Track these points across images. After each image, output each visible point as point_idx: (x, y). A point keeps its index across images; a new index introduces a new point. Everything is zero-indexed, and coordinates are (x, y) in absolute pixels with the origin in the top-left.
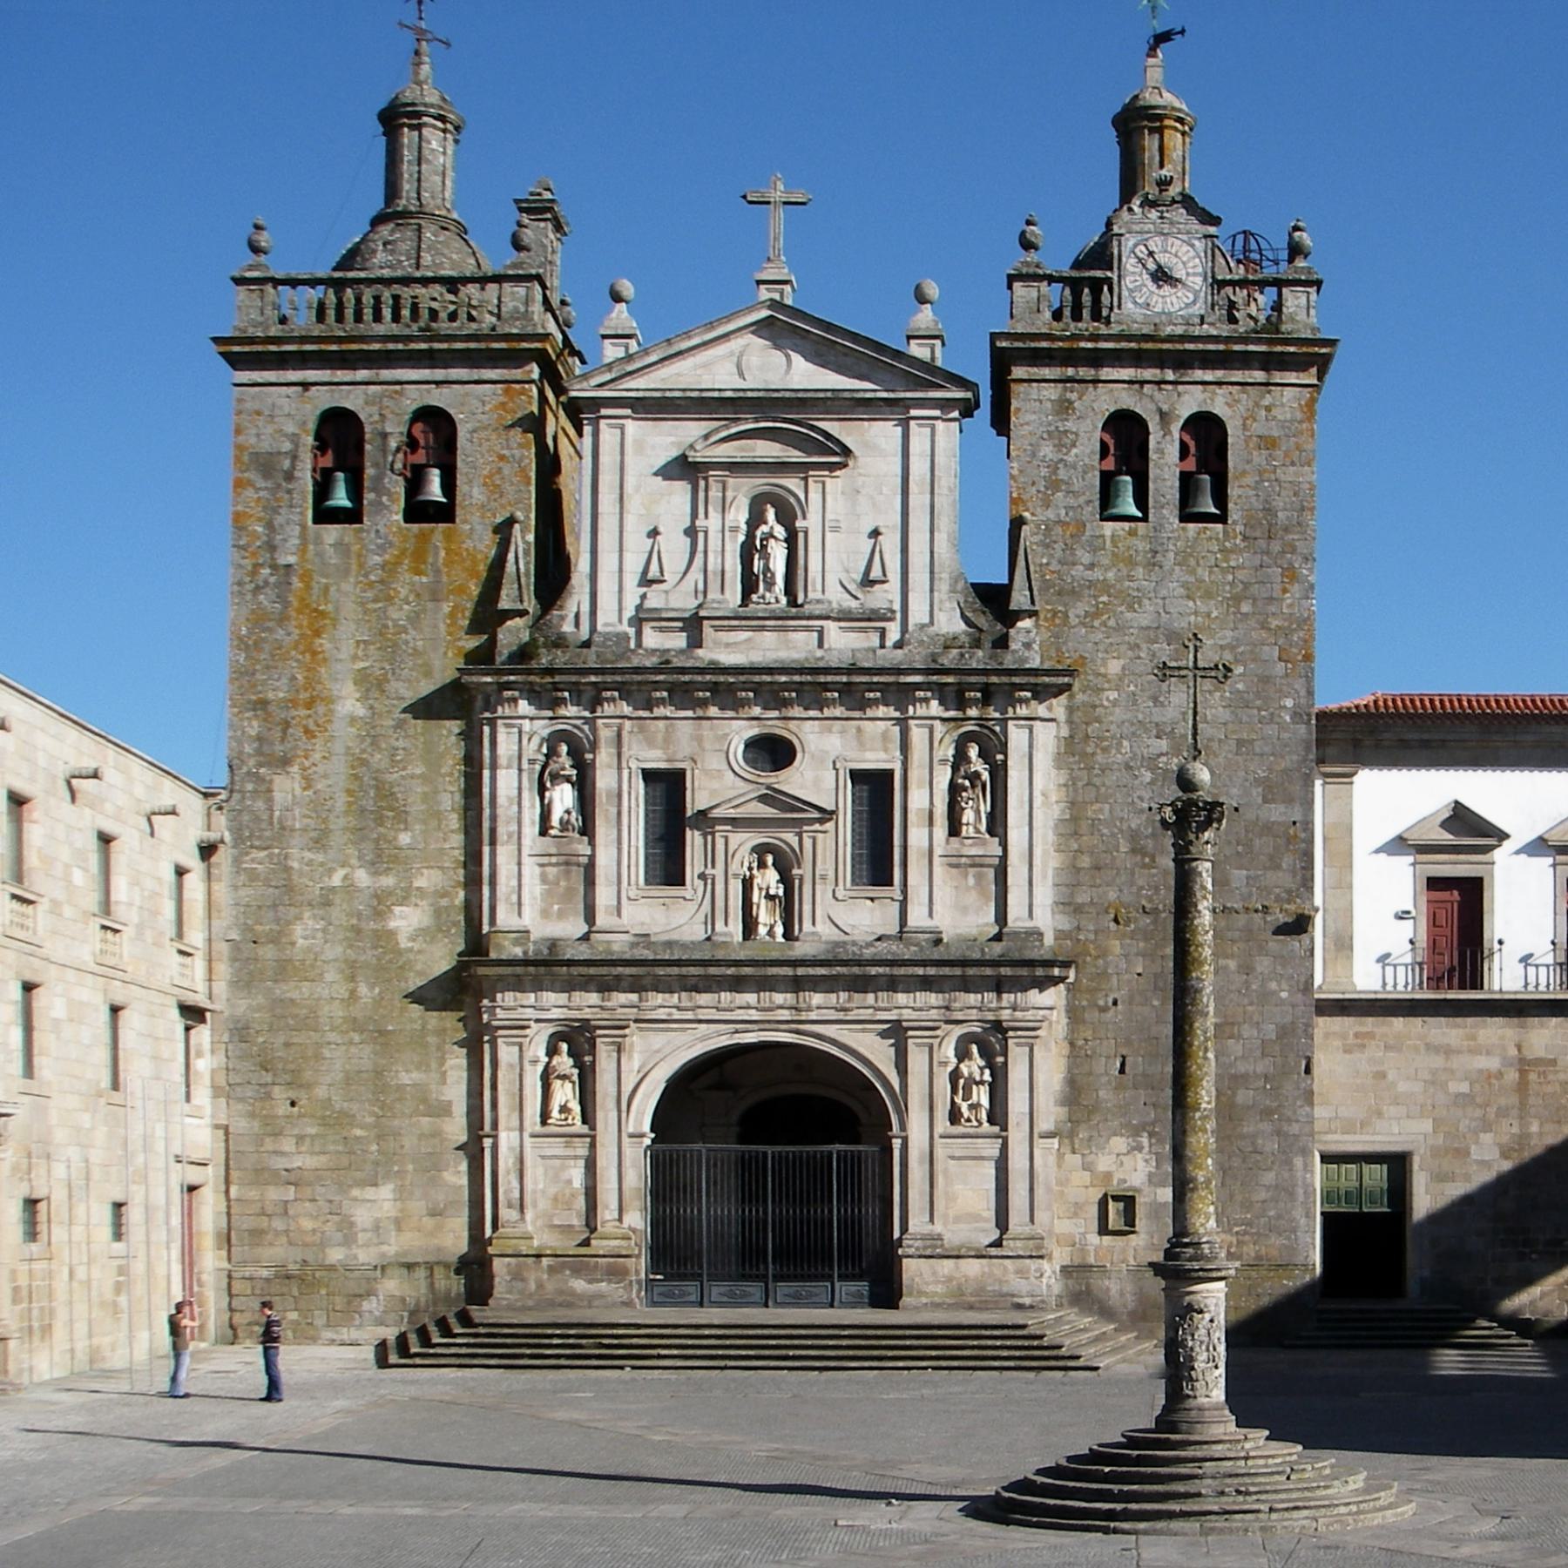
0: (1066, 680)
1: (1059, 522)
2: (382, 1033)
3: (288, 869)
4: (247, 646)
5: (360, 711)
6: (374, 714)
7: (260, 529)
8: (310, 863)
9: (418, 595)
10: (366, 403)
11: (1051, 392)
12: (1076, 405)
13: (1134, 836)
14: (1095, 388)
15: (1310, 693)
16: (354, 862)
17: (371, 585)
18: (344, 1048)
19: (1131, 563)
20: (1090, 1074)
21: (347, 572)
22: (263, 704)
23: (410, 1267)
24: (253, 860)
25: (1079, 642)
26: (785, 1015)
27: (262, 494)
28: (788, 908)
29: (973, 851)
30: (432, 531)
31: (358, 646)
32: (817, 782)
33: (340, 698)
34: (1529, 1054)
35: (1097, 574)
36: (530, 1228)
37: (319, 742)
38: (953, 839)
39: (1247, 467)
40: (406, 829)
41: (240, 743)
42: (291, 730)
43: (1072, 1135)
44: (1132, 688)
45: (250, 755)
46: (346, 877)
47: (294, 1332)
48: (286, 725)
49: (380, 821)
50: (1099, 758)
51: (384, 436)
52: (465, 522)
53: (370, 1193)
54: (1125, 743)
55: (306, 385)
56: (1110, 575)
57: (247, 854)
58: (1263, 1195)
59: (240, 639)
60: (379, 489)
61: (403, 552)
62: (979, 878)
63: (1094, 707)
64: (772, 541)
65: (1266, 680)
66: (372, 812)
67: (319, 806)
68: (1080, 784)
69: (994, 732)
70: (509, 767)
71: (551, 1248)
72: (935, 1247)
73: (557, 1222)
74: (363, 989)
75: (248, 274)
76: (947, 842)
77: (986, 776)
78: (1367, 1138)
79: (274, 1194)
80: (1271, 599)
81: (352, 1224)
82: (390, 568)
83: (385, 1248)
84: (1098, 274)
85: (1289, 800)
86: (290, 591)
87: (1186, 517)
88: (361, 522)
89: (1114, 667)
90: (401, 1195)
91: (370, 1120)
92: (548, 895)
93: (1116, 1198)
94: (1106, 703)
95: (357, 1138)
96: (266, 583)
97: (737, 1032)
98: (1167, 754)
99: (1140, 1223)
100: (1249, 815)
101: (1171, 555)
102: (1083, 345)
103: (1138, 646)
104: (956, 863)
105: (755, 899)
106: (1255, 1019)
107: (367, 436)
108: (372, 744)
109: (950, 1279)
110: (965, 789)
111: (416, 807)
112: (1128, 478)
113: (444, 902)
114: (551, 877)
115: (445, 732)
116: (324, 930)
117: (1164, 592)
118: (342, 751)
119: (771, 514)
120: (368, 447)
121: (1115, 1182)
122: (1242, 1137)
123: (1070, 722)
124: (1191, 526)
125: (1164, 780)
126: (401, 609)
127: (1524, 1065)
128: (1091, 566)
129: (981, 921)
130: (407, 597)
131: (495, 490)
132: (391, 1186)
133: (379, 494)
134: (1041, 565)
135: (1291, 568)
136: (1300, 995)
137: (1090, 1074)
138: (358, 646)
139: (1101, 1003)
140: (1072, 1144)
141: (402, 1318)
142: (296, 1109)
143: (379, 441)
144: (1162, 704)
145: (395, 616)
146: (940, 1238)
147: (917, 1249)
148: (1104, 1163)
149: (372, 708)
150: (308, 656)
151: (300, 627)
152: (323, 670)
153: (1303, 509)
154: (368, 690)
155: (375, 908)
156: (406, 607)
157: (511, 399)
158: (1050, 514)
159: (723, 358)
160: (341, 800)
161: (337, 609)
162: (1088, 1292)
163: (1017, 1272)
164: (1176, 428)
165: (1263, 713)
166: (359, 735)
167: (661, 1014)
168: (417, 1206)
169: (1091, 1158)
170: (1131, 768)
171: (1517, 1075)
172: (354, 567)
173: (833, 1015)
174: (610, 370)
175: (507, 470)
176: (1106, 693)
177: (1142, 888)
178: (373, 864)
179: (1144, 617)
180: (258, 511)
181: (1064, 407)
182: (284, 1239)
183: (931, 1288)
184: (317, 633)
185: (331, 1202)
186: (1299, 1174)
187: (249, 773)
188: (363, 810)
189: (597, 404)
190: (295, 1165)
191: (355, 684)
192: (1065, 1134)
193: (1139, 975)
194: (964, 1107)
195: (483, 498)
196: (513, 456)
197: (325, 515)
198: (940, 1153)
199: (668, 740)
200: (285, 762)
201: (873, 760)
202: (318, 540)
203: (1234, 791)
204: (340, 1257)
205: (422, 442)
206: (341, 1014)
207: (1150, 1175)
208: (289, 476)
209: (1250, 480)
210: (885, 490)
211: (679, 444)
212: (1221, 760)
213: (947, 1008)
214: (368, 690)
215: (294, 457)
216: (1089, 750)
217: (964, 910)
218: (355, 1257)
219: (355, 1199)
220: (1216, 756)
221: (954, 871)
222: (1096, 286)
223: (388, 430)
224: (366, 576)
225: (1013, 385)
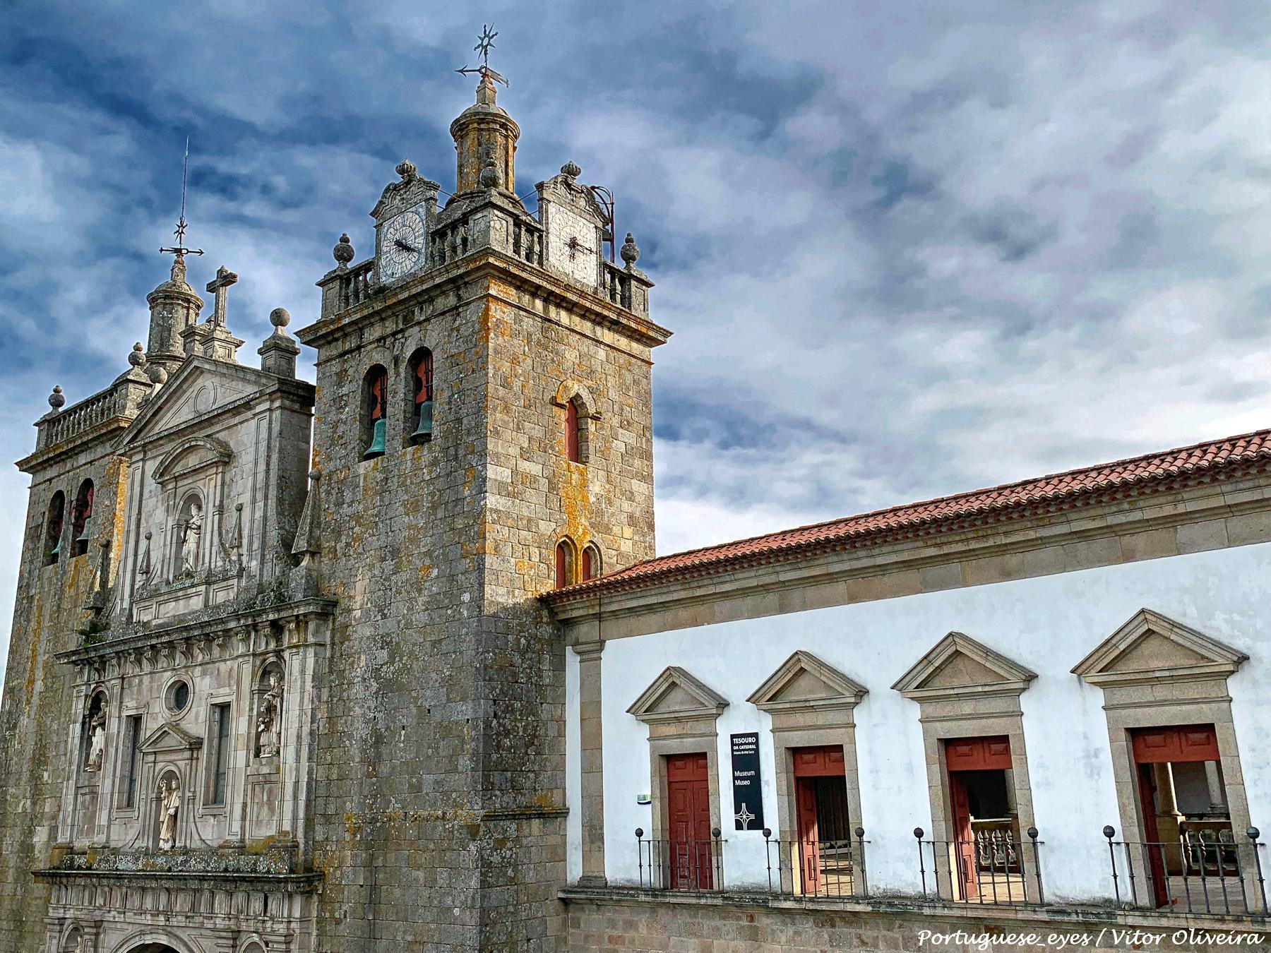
2: (21, 922)
11: (335, 367)
44: (369, 605)
49: (39, 765)
54: (363, 657)
55: (50, 480)
62: (270, 792)
97: (142, 933)
98: (387, 663)
100: (437, 716)
101: (395, 479)
105: (161, 819)
117: (390, 515)
164: (402, 368)
165: (449, 612)
176: (355, 612)
193: (362, 886)
199: (139, 692)
200: (15, 726)
209: (446, 394)
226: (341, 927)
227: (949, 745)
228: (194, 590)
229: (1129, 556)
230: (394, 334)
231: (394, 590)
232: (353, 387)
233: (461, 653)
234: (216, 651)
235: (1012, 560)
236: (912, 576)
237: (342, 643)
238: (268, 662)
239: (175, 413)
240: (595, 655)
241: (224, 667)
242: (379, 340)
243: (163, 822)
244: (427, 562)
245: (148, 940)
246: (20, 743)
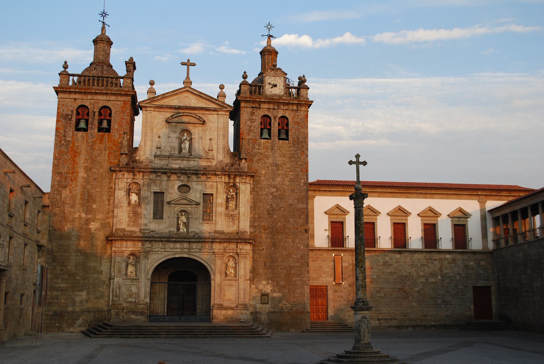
0: (254, 174)
1: (251, 139)
3: (64, 213)
4: (58, 159)
5: (85, 176)
6: (88, 176)
7: (62, 132)
8: (70, 211)
9: (101, 149)
10: (90, 104)
11: (250, 110)
12: (255, 113)
13: (268, 211)
14: (259, 110)
15: (307, 179)
16: (81, 211)
17: (89, 146)
18: (76, 257)
19: (267, 149)
20: (257, 266)
21: (84, 143)
22: (61, 173)
23: (89, 312)
24: (56, 210)
25: (255, 166)
26: (186, 250)
27: (63, 124)
28: (186, 225)
29: (232, 213)
30: (105, 134)
31: (85, 160)
32: (195, 196)
33: (80, 172)
35: (260, 151)
36: (121, 302)
37: (74, 182)
38: (226, 210)
39: (293, 129)
40: (95, 204)
41: (54, 182)
42: (67, 179)
43: (253, 280)
45: (56, 185)
46: (79, 215)
47: (58, 329)
48: (66, 178)
49: (88, 202)
50: (260, 192)
51: (94, 113)
52: (113, 132)
53: (80, 293)
54: (266, 189)
55: (75, 99)
56: (263, 151)
57: (54, 209)
58: (297, 295)
59: (56, 157)
60: (92, 124)
61: (97, 140)
62: (233, 219)
63: (259, 181)
64: (186, 141)
65: (297, 176)
66: (86, 200)
67: (73, 198)
68: (256, 198)
69: (237, 186)
70: (122, 190)
71: (126, 307)
72: (221, 307)
73: (128, 301)
74: (82, 242)
75: (63, 73)
76: (225, 211)
77: (234, 196)
78: (318, 282)
79: (55, 293)
80: (299, 158)
81: (75, 301)
82: (94, 143)
83: (83, 307)
84: (260, 85)
85: (303, 203)
86: (69, 147)
87: (279, 139)
88: (87, 131)
89: (263, 172)
90: (88, 294)
91: (81, 275)
92: (130, 220)
93: (264, 295)
94: (262, 180)
95: (78, 279)
96: (63, 144)
99: (270, 302)
101: (276, 147)
102: (257, 100)
103: (269, 167)
104: (228, 216)
105: (180, 223)
106: (296, 253)
107: (90, 112)
108: (87, 183)
109: (224, 315)
110: (230, 198)
111: (98, 199)
112: (266, 130)
113: (103, 222)
114: (130, 216)
115: (106, 181)
116: (73, 228)
117: (275, 155)
118: (80, 185)
119: (185, 134)
120: (90, 114)
121: (263, 292)
122: (293, 281)
123: (253, 184)
124: (281, 141)
125: (275, 198)
126: (96, 152)
128: (258, 149)
129: (233, 229)
130: (98, 149)
131: (120, 125)
132: (85, 292)
133: (92, 125)
134: (247, 148)
135: (303, 151)
136: (306, 248)
137: (257, 266)
138: (85, 160)
139: (260, 249)
140: (253, 282)
141: (86, 325)
142: (62, 272)
143: (93, 113)
144: (274, 181)
145: (95, 153)
146: (222, 304)
147: (217, 308)
148: (261, 287)
149: (88, 175)
150: (73, 162)
151: (71, 155)
152: (76, 166)
153: (305, 138)
154: (87, 171)
155: (86, 223)
156: (98, 152)
157: (125, 105)
158: (249, 137)
159: (176, 99)
160: (79, 197)
161: (80, 151)
162: (257, 318)
163: (240, 314)
164: (277, 119)
166: (84, 181)
167: (157, 250)
168: (92, 297)
170: (267, 195)
171: (352, 267)
172: (85, 142)
173: (198, 250)
174: (149, 100)
175: (123, 121)
177: (269, 222)
178: (86, 212)
179: (270, 161)
180: (62, 128)
181: (253, 114)
182: (57, 305)
183: (220, 317)
184: (75, 157)
185: (70, 295)
187: (56, 189)
188: (84, 199)
189: (146, 107)
190: (61, 286)
191: (84, 169)
192: (252, 280)
194: (228, 273)
195: (117, 127)
196: (125, 118)
197: (78, 129)
200: (65, 187)
201: (209, 191)
202: (77, 135)
203: (291, 201)
204: (72, 310)
205: (103, 114)
206: (76, 248)
207: (271, 290)
208: (70, 119)
209: (294, 131)
210: (212, 130)
211: (165, 118)
212: (288, 193)
213: (225, 249)
214: (87, 171)
215: (72, 116)
216: (258, 190)
217: (229, 226)
218: (75, 310)
219: (76, 295)
220: (286, 192)
221: (227, 218)
222: (260, 87)
223: (95, 111)
224: (88, 144)
225: (241, 108)
226: (262, 251)
227: (394, 223)
228: (193, 159)
229: (426, 198)
230: (274, 109)
231: (277, 175)
232: (257, 118)
233: (301, 193)
234: (203, 178)
235: (408, 195)
236: (391, 195)
237: (258, 185)
238: (229, 185)
239: (171, 100)
240: (312, 199)
241: (207, 183)
242: (268, 109)
243: (180, 224)
244: (289, 170)
245: (178, 256)
246: (71, 193)
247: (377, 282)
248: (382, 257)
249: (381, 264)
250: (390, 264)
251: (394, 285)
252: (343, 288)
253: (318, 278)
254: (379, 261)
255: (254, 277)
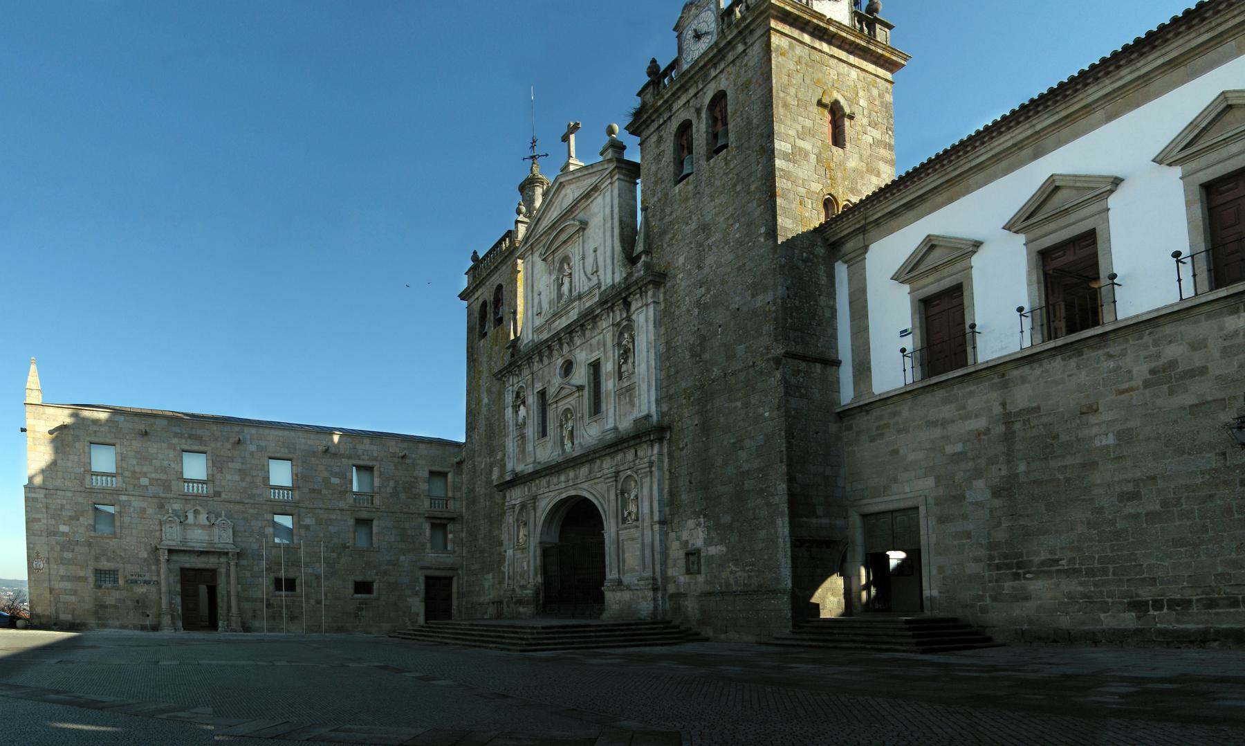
34: (1012, 409)
43: (672, 521)
78: (886, 498)
89: (681, 260)
121: (690, 546)
127: (1008, 418)
148: (685, 535)
169: (678, 534)
171: (1003, 428)
186: (780, 530)
194: (626, 513)
198: (621, 538)
245: (564, 496)
247: (1119, 458)
248: (1143, 353)
249: (1138, 382)
250: (1192, 370)
251: (1224, 454)
252: (972, 504)
253: (886, 488)
254: (1129, 372)
255: (672, 515)
